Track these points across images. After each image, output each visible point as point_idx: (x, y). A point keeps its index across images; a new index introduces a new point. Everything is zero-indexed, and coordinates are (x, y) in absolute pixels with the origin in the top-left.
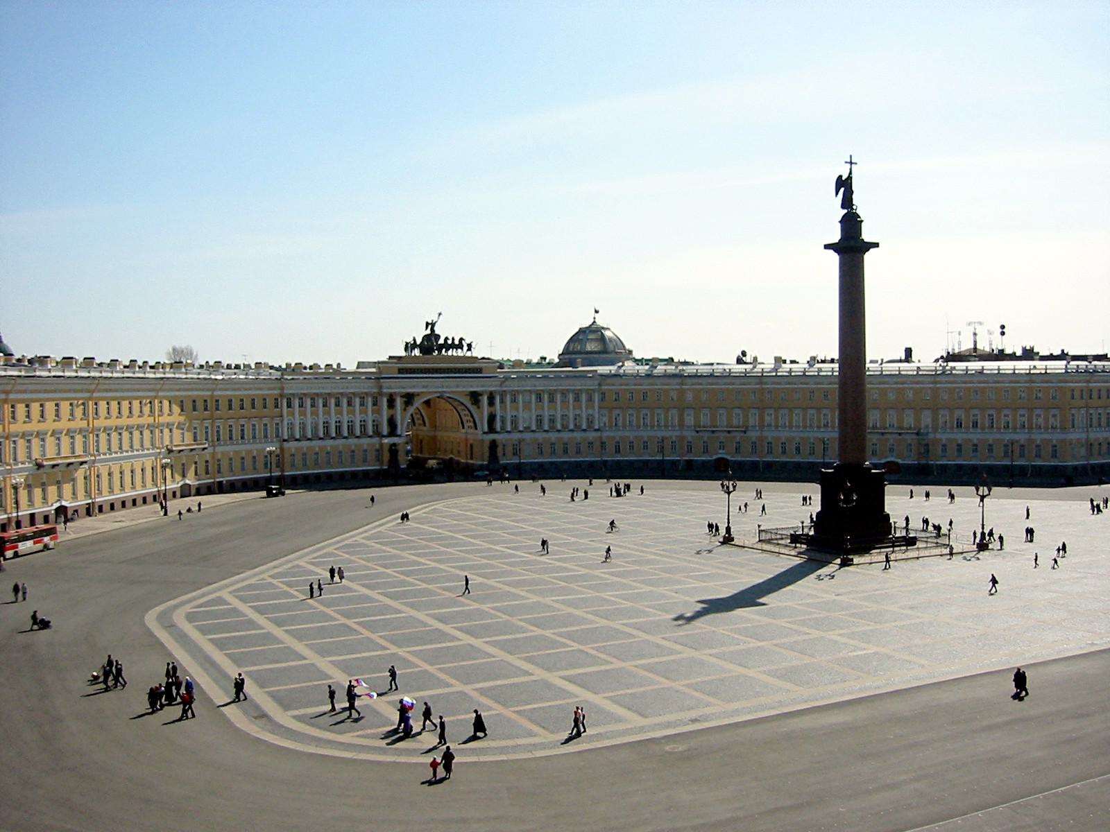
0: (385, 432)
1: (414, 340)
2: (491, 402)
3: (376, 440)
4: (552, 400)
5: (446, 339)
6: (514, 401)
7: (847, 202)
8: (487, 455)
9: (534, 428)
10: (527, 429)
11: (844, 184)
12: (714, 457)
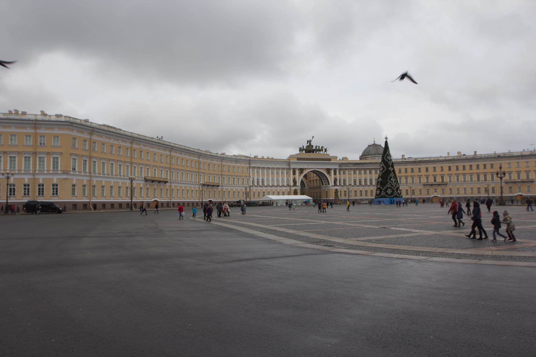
0: (292, 185)
2: (335, 174)
3: (288, 188)
5: (316, 146)
8: (334, 195)
10: (350, 185)
12: (432, 196)
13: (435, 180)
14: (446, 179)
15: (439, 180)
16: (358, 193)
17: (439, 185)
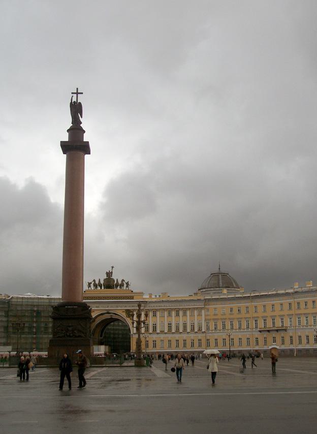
1: (94, 281)
4: (178, 315)
6: (155, 315)
7: (76, 122)
9: (166, 331)
10: (162, 332)
11: (76, 109)
12: (270, 347)
13: (274, 323)
14: (287, 323)
15: (278, 324)
16: (174, 344)
17: (277, 331)
